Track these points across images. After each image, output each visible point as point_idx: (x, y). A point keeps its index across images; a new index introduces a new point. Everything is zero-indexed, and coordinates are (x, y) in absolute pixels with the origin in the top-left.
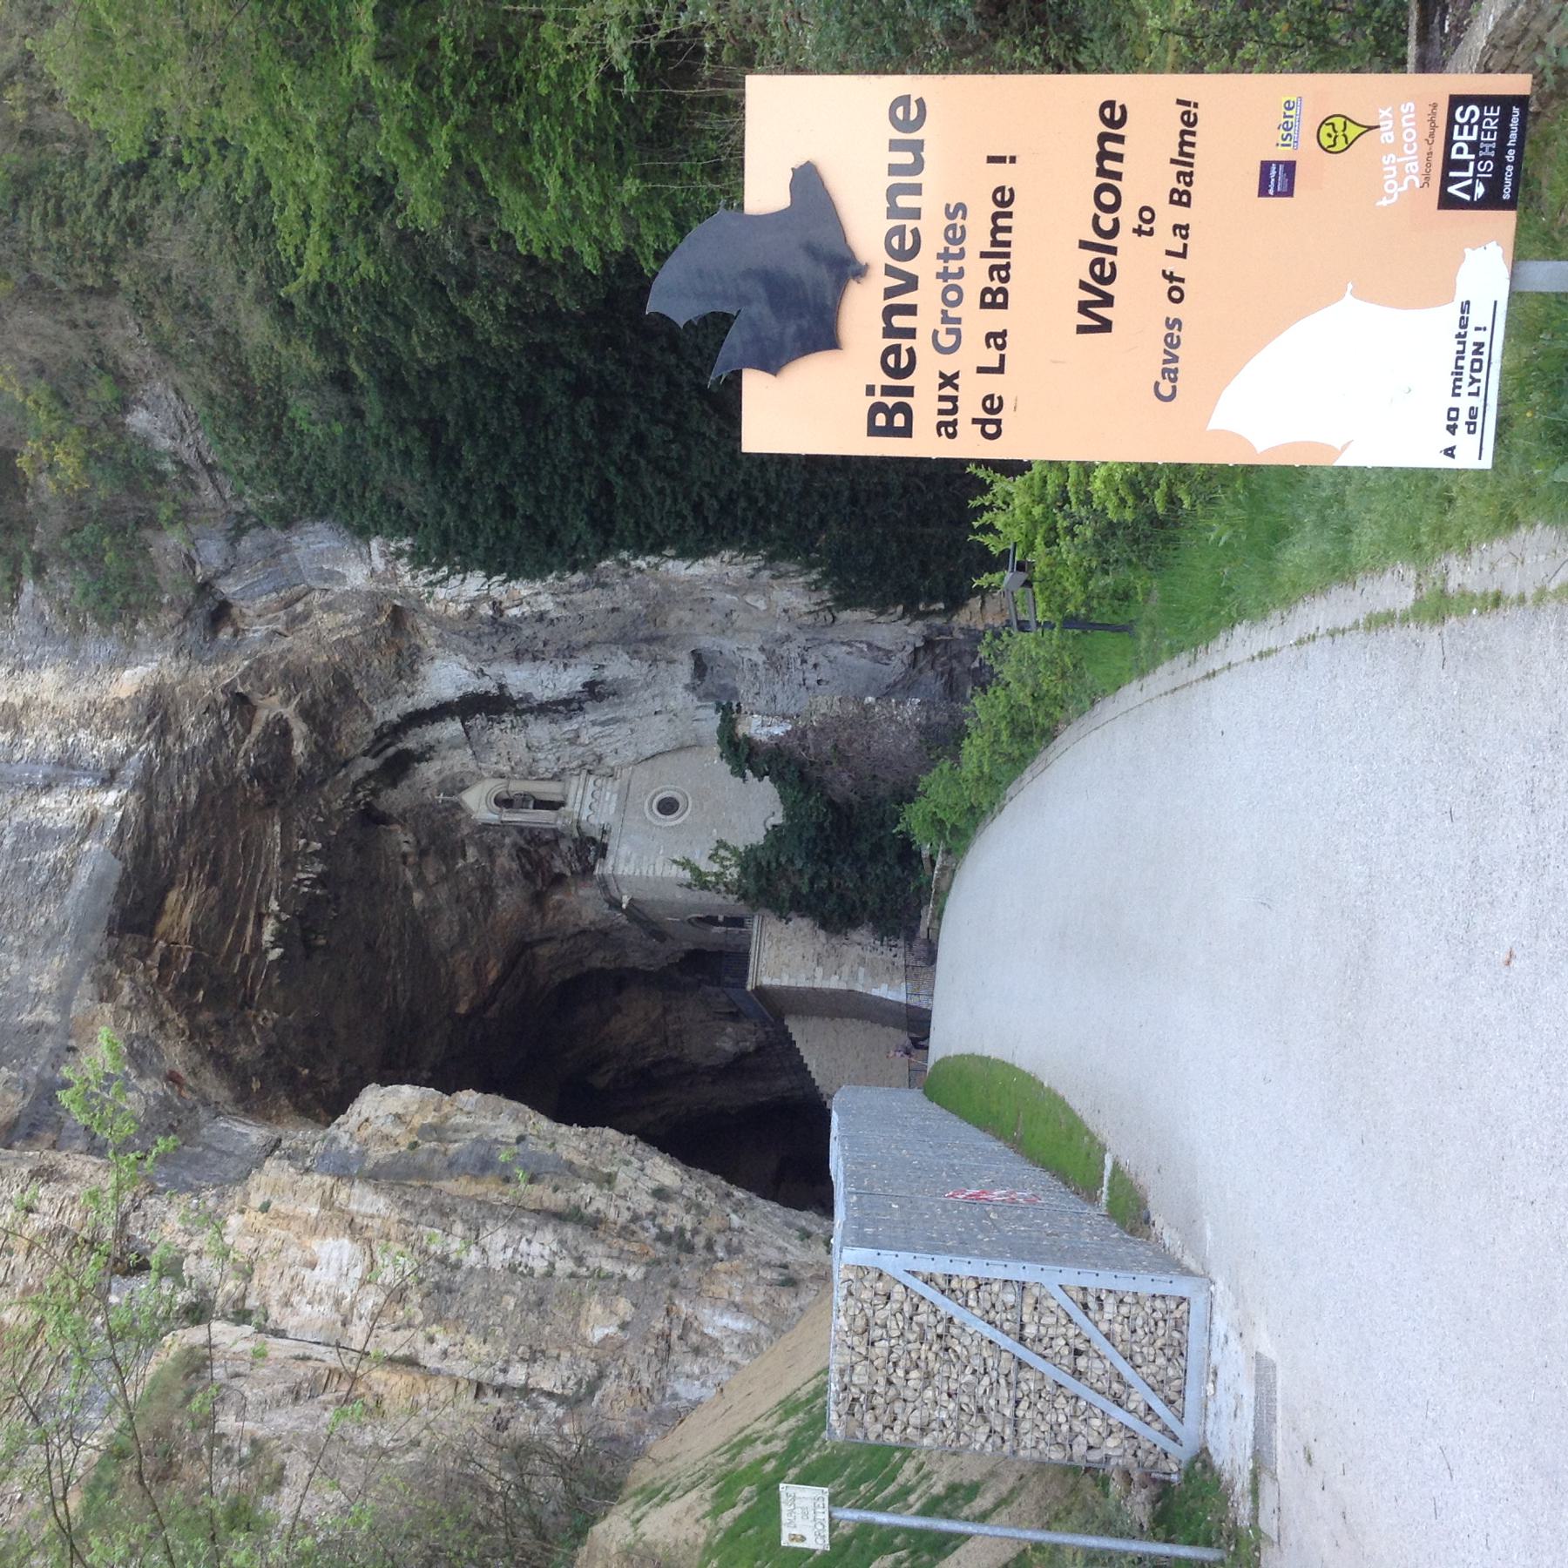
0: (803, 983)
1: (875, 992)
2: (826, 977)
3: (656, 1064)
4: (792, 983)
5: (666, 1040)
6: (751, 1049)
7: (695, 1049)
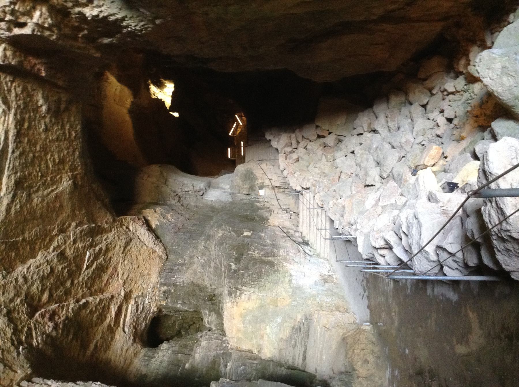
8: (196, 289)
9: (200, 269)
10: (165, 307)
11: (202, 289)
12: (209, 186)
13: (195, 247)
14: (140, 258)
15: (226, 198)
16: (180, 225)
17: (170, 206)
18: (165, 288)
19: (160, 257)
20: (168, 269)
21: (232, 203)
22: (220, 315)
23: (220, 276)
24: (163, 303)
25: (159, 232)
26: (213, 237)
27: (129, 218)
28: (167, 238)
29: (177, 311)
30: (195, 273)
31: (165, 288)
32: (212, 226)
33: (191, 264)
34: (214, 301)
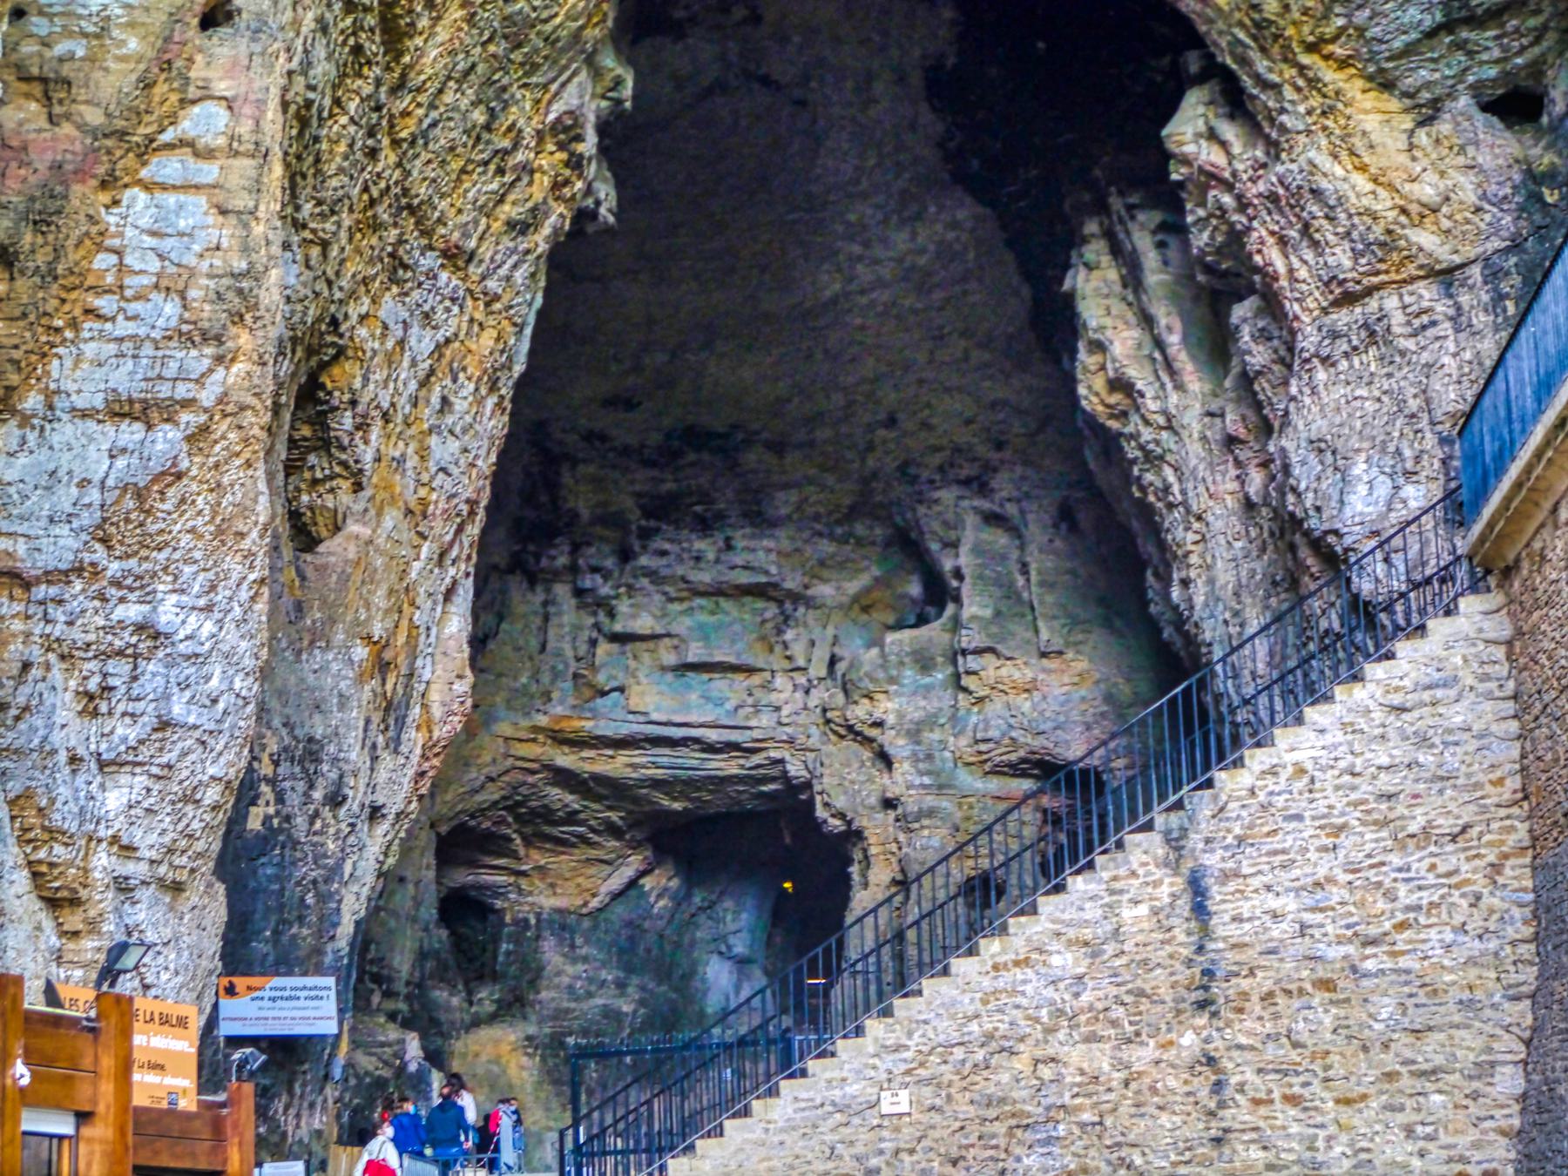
3: (1272, 305)
5: (1348, 299)
6: (1365, 586)
7: (1324, 404)
8: (534, 974)
9: (566, 980)
10: (502, 924)
11: (534, 984)
12: (742, 962)
13: (604, 965)
14: (580, 880)
15: (713, 1004)
16: (647, 925)
17: (688, 896)
18: (533, 921)
19: (585, 904)
20: (563, 924)
21: (702, 1014)
22: (493, 1018)
23: (555, 1018)
24: (508, 919)
25: (633, 893)
26: (622, 995)
27: (648, 853)
28: (620, 910)
29: (496, 940)
30: (559, 973)
31: (533, 921)
32: (643, 988)
33: (574, 961)
34: (513, 1006)
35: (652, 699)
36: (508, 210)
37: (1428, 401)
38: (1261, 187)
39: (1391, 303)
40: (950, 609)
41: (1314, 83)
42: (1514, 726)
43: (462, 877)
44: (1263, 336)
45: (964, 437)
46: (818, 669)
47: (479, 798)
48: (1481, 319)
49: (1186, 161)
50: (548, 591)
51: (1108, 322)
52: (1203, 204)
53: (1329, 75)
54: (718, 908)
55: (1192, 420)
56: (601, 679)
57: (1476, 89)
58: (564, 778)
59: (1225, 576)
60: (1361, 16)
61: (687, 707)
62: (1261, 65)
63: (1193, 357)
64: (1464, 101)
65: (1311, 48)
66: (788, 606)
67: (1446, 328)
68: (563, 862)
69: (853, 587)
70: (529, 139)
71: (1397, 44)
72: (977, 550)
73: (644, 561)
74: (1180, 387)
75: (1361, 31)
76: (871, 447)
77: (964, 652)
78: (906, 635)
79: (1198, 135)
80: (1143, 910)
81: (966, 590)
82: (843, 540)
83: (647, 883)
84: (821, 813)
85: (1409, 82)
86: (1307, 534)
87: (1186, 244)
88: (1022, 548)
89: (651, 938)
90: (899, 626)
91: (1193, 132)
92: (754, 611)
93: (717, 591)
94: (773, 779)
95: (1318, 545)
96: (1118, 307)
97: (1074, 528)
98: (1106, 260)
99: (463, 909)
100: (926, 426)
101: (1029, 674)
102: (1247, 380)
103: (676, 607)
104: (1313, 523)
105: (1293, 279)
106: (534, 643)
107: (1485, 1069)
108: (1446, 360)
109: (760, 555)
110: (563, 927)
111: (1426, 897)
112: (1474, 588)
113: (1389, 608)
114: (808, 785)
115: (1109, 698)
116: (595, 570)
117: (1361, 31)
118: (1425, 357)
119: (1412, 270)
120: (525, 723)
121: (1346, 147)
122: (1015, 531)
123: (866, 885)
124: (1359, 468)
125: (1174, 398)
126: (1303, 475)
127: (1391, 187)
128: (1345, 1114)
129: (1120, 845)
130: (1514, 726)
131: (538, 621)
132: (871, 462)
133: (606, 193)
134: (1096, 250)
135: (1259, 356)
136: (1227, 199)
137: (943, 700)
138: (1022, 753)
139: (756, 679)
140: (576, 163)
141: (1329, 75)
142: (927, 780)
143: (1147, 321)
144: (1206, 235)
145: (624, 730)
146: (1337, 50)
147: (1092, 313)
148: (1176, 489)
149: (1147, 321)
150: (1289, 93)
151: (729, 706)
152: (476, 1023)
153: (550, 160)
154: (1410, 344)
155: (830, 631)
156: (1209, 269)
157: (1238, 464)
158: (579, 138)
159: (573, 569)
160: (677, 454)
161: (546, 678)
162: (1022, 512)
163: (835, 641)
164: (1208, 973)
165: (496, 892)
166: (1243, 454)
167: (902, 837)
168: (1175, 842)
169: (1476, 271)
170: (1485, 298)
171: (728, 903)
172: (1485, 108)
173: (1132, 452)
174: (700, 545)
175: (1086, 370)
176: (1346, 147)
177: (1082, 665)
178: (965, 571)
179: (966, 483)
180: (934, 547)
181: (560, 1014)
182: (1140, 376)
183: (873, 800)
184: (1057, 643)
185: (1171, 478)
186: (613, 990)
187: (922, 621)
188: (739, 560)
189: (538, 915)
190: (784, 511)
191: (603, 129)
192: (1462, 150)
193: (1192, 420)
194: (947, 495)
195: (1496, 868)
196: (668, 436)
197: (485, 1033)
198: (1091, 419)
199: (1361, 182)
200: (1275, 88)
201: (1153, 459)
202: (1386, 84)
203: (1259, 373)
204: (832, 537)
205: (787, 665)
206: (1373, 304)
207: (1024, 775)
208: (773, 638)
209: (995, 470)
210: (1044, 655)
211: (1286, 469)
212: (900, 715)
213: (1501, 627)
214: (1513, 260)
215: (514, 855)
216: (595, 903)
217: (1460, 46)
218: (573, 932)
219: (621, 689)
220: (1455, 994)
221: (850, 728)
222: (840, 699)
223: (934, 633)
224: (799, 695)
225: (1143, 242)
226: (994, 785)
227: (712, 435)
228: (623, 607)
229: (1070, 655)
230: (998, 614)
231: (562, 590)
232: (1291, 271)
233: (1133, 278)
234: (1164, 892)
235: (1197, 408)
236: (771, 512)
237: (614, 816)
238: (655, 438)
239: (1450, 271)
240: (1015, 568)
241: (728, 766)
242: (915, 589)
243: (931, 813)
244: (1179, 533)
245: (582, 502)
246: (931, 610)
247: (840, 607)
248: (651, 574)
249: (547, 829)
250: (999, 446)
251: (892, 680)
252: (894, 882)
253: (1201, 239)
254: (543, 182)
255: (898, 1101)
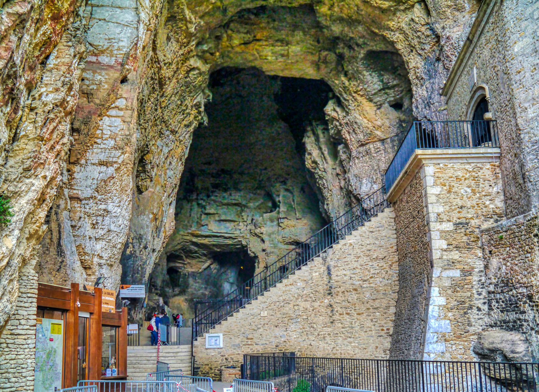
0: (434, 209)
1: (435, 291)
2: (444, 234)
3: (346, 146)
4: (431, 199)
5: (362, 145)
6: (365, 206)
7: (357, 167)
8: (187, 286)
9: (194, 287)
10: (181, 275)
12: (232, 284)
13: (202, 284)
15: (225, 292)
17: (221, 269)
20: (193, 275)
21: (223, 295)
25: (209, 268)
27: (212, 260)
28: (206, 272)
29: (179, 278)
30: (192, 285)
32: (210, 289)
34: (183, 292)
35: (214, 227)
36: (185, 122)
37: (379, 167)
38: (345, 121)
39: (371, 146)
40: (277, 209)
41: (356, 100)
42: (395, 236)
43: (172, 265)
44: (344, 152)
45: (280, 172)
46: (249, 221)
47: (176, 248)
48: (390, 150)
49: (329, 115)
50: (191, 203)
51: (312, 149)
52: (332, 124)
53: (359, 98)
54: (227, 272)
55: (329, 170)
56: (202, 223)
57: (389, 102)
58: (194, 244)
59: (336, 203)
60: (366, 86)
61: (221, 229)
62: (345, 96)
63: (330, 157)
64: (387, 105)
65: (355, 92)
66: (243, 208)
67: (383, 152)
68: (194, 262)
69: (257, 204)
70: (189, 108)
71: (373, 92)
72: (284, 196)
73: (212, 198)
74: (327, 163)
75: (365, 89)
76: (261, 174)
77: (280, 218)
78: (268, 214)
79: (332, 110)
80: (317, 274)
81: (281, 205)
82: (255, 194)
83: (212, 266)
84: (249, 252)
85: (375, 100)
86: (353, 194)
87: (329, 133)
88: (293, 196)
89: (212, 278)
90: (266, 212)
91: (330, 109)
92: (236, 209)
93: (228, 204)
94: (239, 245)
95: (355, 197)
96: (314, 146)
97: (304, 192)
98: (312, 135)
99: (172, 272)
100: (273, 170)
101: (294, 223)
102: (341, 162)
103: (219, 207)
104: (354, 192)
105: (351, 141)
106: (188, 215)
107: (388, 307)
108: (383, 158)
109: (237, 197)
110: (193, 275)
111: (377, 271)
112: (388, 207)
113: (370, 211)
114: (246, 246)
115: (311, 229)
116: (202, 199)
117: (365, 89)
118: (378, 158)
119: (376, 139)
120: (186, 232)
121: (363, 114)
122: (291, 193)
123: (258, 268)
124: (364, 181)
125: (326, 165)
126: (352, 182)
127: (371, 122)
128: (359, 317)
129: (313, 260)
130: (395, 236)
131: (189, 210)
132: (261, 178)
133: (206, 119)
134: (310, 134)
135: (344, 157)
136: (337, 124)
137: (276, 228)
138: (292, 240)
139: (236, 223)
140: (199, 113)
141: (359, 98)
142: (272, 245)
143: (320, 149)
144: (333, 131)
145: (207, 234)
146: (361, 93)
147: (309, 147)
148: (326, 184)
149: (320, 149)
150: (351, 102)
151: (230, 229)
152: (175, 296)
153: (194, 112)
154: (375, 155)
155: (252, 213)
156: (334, 138)
157: (339, 179)
158: (200, 107)
159: (197, 199)
160: (220, 175)
161: (191, 222)
162: (293, 189)
163: (253, 215)
164: (331, 287)
165: (179, 267)
166: (340, 177)
167: (266, 258)
168: (324, 260)
169: (389, 140)
170: (391, 146)
171: (229, 271)
172: (391, 106)
173: (317, 176)
174: (225, 194)
175: (307, 159)
176: (363, 114)
177: (305, 221)
178: (281, 201)
179: (282, 182)
180: (274, 196)
181: (193, 294)
182: (318, 160)
183: (261, 250)
184: (300, 217)
185: (324, 181)
186: (204, 289)
187: (271, 211)
188: (233, 198)
189: (188, 273)
190: (243, 187)
191: (205, 106)
192: (386, 115)
193: (329, 170)
194: (278, 185)
195: (391, 265)
196: (218, 171)
197: (177, 298)
198: (308, 170)
199: (366, 121)
200: (348, 100)
201: (321, 178)
202: (371, 100)
203: (344, 160)
204: (252, 193)
205: (243, 220)
206: (368, 146)
207: (293, 245)
208: (239, 215)
209: (287, 180)
210: (297, 219)
211: (349, 181)
212: (267, 231)
213: (393, 215)
214: (396, 138)
215: (184, 261)
216: (200, 271)
217: (386, 93)
218: (196, 277)
219: (207, 225)
220: (382, 292)
221: (256, 234)
222: (254, 228)
223: (274, 214)
224: (245, 227)
225: (320, 132)
226: (287, 247)
227: (228, 171)
228: (208, 207)
229: (303, 219)
230: (288, 210)
231: (194, 203)
232: (351, 139)
233: (317, 140)
234: (322, 270)
235: (331, 167)
236: (239, 187)
237: (205, 252)
238: (215, 171)
239: (383, 140)
240: (291, 200)
241: (229, 242)
242: (270, 205)
243: (273, 252)
244: (326, 194)
245: (199, 185)
246: (273, 209)
247: (254, 208)
248: (215, 201)
249: (190, 255)
250: (289, 175)
251: (265, 224)
252: (265, 267)
253: (332, 132)
254: (192, 118)
255: (265, 314)
